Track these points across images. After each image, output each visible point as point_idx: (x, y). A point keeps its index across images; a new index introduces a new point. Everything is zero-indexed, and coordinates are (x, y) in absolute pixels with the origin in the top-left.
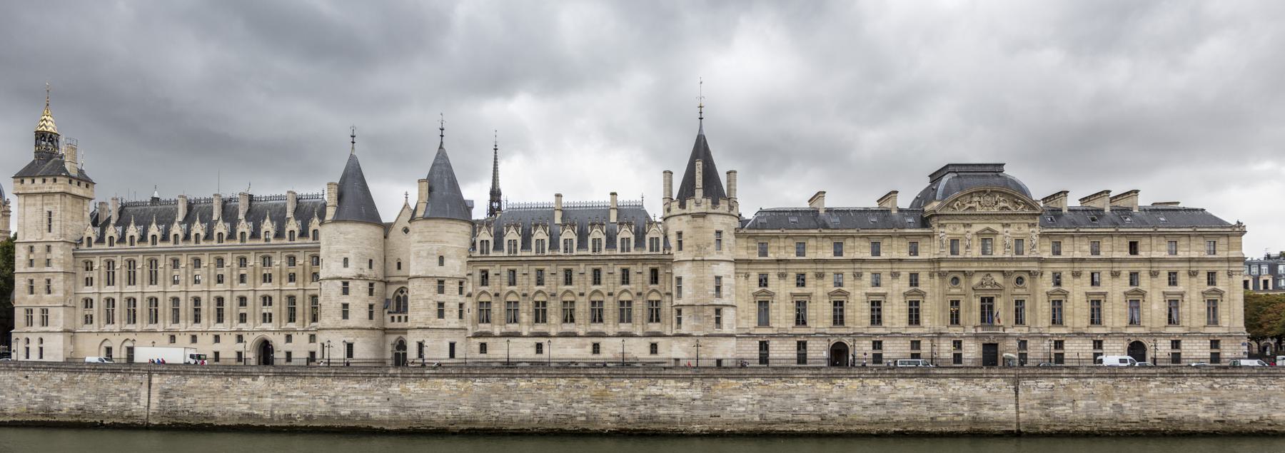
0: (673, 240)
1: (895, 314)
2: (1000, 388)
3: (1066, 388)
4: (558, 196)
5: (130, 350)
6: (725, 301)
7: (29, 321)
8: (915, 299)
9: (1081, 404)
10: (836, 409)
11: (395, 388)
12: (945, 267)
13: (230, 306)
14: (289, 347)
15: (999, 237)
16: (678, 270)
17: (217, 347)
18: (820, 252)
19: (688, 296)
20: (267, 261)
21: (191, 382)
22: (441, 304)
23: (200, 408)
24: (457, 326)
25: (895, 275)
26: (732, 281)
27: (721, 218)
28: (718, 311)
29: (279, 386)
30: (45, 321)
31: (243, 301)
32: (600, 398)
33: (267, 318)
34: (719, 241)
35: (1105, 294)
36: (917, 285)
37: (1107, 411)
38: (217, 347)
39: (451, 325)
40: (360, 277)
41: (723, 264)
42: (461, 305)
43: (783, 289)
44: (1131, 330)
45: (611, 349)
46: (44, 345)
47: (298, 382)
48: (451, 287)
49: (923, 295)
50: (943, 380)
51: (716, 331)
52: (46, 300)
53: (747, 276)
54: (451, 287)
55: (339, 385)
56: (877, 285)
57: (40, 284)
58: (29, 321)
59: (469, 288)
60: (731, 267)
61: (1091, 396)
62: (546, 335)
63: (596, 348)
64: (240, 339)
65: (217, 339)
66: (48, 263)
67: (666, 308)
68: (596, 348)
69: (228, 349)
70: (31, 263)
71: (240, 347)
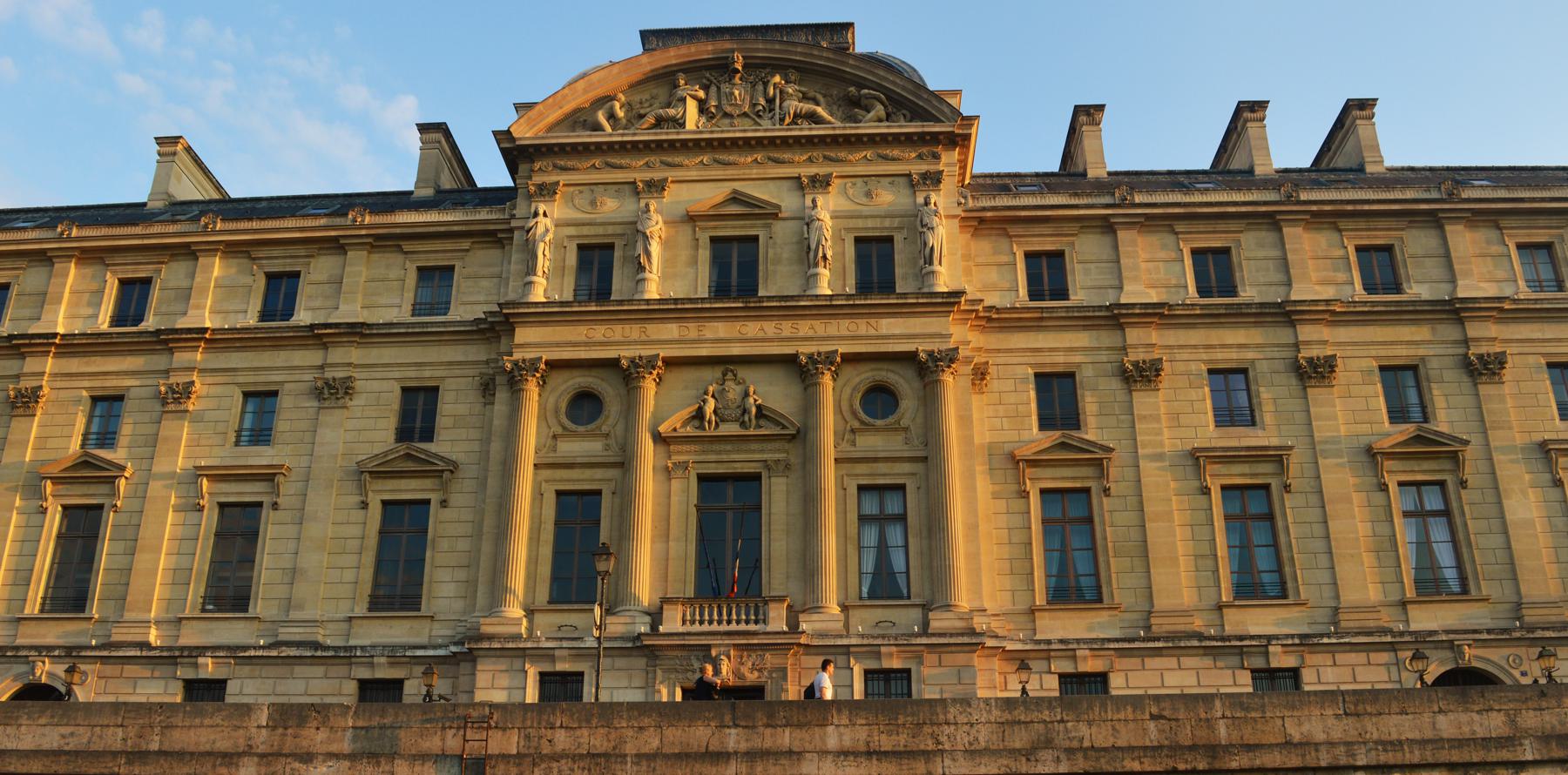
8: (408, 490)
15: (783, 231)
25: (332, 392)
35: (1277, 458)
36: (428, 435)
44: (1426, 619)
49: (443, 472)
56: (261, 435)
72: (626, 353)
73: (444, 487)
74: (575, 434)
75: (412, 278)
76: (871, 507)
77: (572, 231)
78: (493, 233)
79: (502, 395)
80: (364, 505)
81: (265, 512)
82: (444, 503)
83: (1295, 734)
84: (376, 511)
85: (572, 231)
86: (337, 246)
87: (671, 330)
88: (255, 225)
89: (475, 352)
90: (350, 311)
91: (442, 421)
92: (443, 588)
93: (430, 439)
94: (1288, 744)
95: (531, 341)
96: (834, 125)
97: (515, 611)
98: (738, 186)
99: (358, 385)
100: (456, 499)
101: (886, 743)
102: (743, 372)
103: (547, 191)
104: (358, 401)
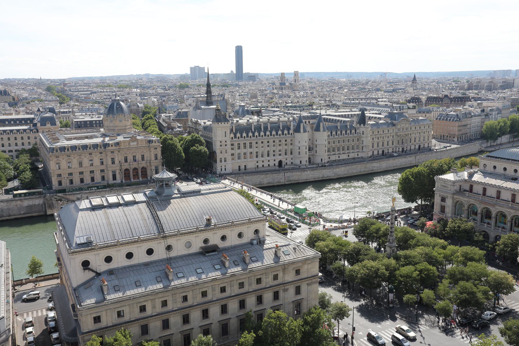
0: (362, 133)
1: (390, 143)
5: (245, 166)
7: (221, 161)
11: (335, 170)
12: (398, 134)
13: (271, 153)
14: (286, 161)
16: (362, 139)
17: (269, 163)
19: (365, 144)
20: (280, 141)
21: (294, 174)
23: (296, 179)
29: (312, 172)
30: (225, 161)
31: (274, 151)
32: (365, 168)
33: (280, 155)
38: (269, 163)
43: (376, 140)
45: (352, 155)
46: (226, 167)
47: (316, 171)
52: (226, 155)
55: (324, 171)
57: (224, 151)
58: (221, 161)
62: (340, 154)
63: (349, 156)
64: (275, 160)
65: (263, 162)
66: (226, 145)
67: (361, 146)
68: (349, 156)
69: (272, 163)
70: (221, 146)
71: (275, 162)
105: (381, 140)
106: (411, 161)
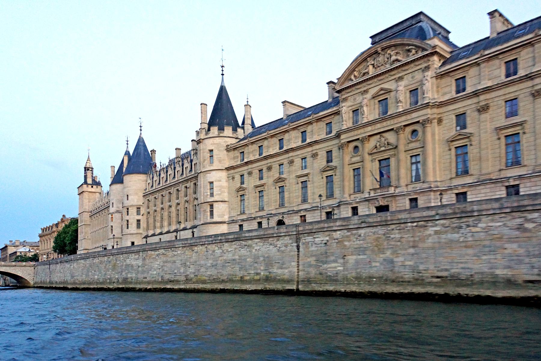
2: (286, 246)
3: (340, 242)
4: (178, 149)
6: (216, 198)
8: (329, 173)
9: (352, 259)
10: (193, 271)
18: (271, 150)
22: (138, 221)
24: (135, 232)
25: (315, 156)
26: (224, 183)
27: (211, 140)
28: (212, 206)
34: (212, 156)
37: (377, 268)
39: (132, 232)
40: (118, 212)
41: (214, 172)
42: (138, 221)
43: (251, 182)
48: (133, 211)
50: (250, 242)
51: (209, 220)
53: (233, 178)
54: (133, 211)
59: (143, 210)
60: (224, 174)
61: (360, 250)
72: (360, 137)
73: (335, 172)
74: (355, 156)
75: (325, 126)
76: (414, 160)
77: (351, 108)
78: (336, 113)
79: (341, 150)
80: (323, 178)
81: (308, 182)
82: (335, 175)
83: (400, 217)
84: (325, 179)
85: (351, 108)
86: (310, 123)
87: (369, 128)
88: (297, 123)
89: (336, 141)
90: (316, 138)
91: (333, 158)
92: (337, 192)
93: (332, 162)
94: (398, 219)
95: (344, 138)
96: (404, 60)
97: (346, 195)
98: (382, 86)
99: (319, 153)
100: (337, 174)
101: (344, 224)
102: (384, 134)
103: (345, 100)
104: (319, 156)
105: (269, 178)
106: (269, 262)
